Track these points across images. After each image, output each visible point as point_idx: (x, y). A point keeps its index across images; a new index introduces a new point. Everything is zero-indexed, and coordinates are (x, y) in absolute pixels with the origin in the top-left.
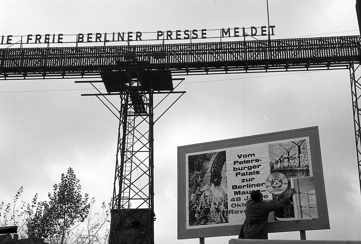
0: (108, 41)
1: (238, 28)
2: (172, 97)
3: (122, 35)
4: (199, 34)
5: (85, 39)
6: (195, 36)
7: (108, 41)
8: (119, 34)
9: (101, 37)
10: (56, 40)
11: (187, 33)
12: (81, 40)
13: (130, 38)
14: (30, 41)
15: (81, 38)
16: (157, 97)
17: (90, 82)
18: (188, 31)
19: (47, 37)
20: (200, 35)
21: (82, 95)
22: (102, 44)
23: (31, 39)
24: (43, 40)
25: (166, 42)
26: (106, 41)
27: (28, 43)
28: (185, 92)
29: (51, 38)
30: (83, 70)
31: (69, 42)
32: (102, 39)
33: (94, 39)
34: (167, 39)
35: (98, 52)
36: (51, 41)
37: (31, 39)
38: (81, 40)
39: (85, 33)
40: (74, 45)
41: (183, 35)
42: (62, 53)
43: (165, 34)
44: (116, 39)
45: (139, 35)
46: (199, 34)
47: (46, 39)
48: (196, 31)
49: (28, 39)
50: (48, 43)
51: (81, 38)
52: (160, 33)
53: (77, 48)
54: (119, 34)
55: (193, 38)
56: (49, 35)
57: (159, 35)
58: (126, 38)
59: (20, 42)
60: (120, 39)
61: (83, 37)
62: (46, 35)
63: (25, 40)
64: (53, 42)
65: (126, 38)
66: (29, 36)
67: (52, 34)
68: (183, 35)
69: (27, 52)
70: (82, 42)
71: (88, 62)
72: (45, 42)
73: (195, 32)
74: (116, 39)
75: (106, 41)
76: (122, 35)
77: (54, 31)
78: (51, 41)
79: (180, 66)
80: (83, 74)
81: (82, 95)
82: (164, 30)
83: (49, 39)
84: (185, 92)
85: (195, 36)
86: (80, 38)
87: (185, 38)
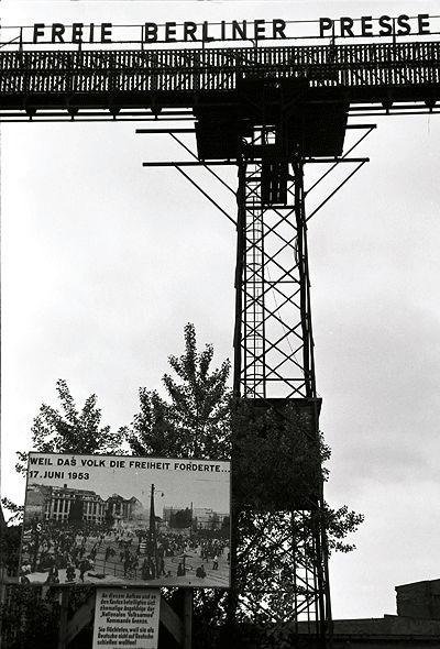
0: (212, 39)
1: (262, 22)
2: (344, 169)
3: (241, 26)
4: (414, 25)
5: (161, 34)
6: (404, 29)
7: (212, 39)
8: (235, 24)
9: (195, 30)
10: (97, 37)
11: (385, 21)
12: (151, 37)
13: (260, 34)
14: (40, 39)
15: (151, 33)
16: (312, 171)
17: (170, 131)
18: (388, 19)
19: (78, 29)
20: (415, 28)
21: (145, 164)
22: (198, 45)
23: (42, 34)
24: (68, 35)
25: (339, 42)
26: (206, 39)
27: (35, 42)
28: (368, 160)
29: (86, 32)
30: (156, 102)
31: (126, 37)
32: (199, 34)
33: (180, 34)
34: (343, 36)
35: (192, 63)
36: (86, 37)
37: (42, 34)
38: (151, 37)
39: (160, 21)
40: (138, 47)
41: (376, 28)
42: (110, 65)
43: (338, 25)
44: (229, 34)
45: (279, 27)
46: (414, 25)
47: (75, 33)
48: (407, 18)
49: (37, 34)
50: (80, 42)
51: (151, 33)
52: (325, 24)
53: (143, 55)
54: (235, 24)
55: (401, 33)
56: (81, 25)
57: (323, 28)
58: (250, 33)
59: (18, 40)
60: (238, 36)
61: (156, 30)
62: (75, 26)
63: (28, 35)
64: (91, 41)
65: (250, 33)
66: (37, 26)
67: (87, 23)
68: (376, 28)
69: (35, 60)
70: (154, 41)
71: (169, 83)
72: (74, 41)
73: (403, 21)
74: (229, 34)
75: (206, 39)
76: (241, 26)
77: (91, 16)
78: (86, 37)
79: (366, 94)
80: (156, 112)
81: (145, 164)
82: (335, 16)
83: (80, 33)
84: (368, 160)
85: (404, 29)
86: (150, 30)
87: (382, 34)
